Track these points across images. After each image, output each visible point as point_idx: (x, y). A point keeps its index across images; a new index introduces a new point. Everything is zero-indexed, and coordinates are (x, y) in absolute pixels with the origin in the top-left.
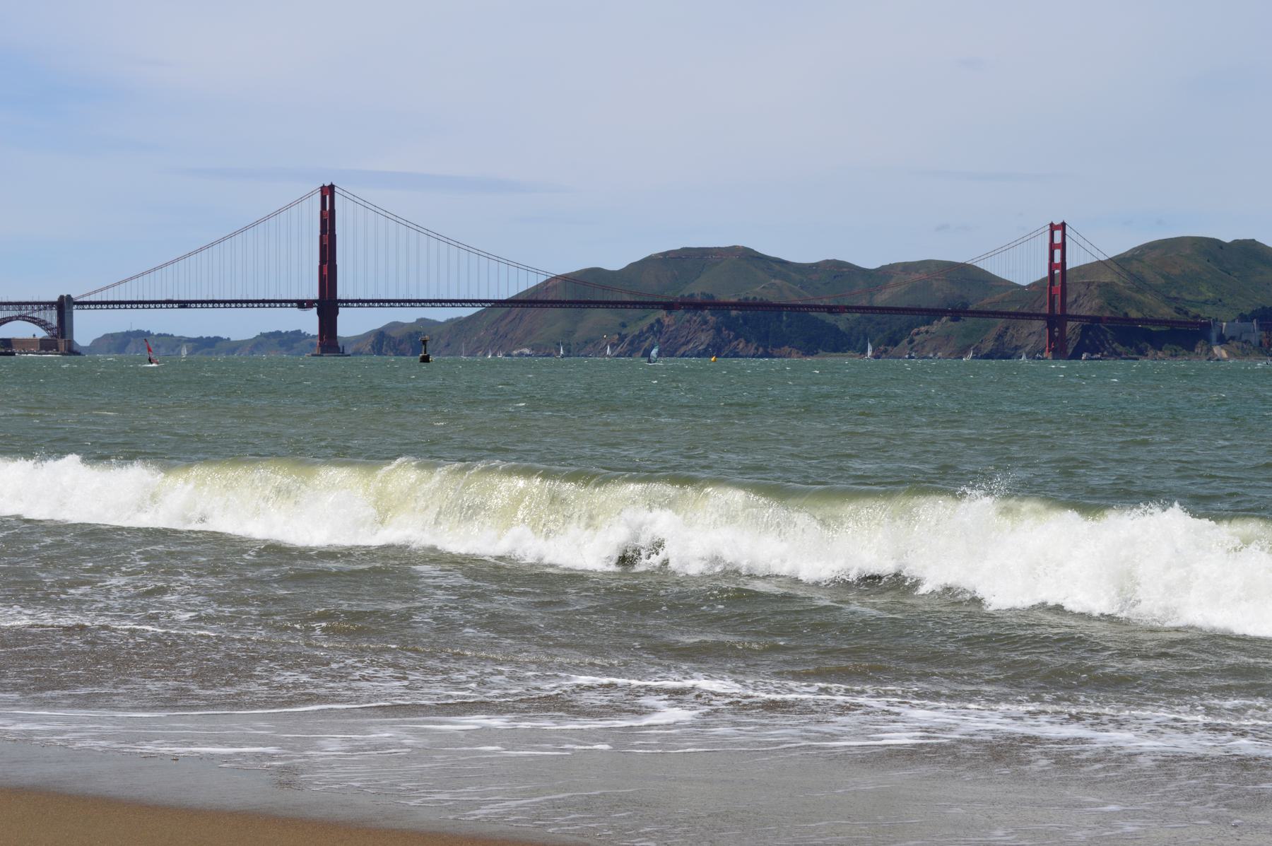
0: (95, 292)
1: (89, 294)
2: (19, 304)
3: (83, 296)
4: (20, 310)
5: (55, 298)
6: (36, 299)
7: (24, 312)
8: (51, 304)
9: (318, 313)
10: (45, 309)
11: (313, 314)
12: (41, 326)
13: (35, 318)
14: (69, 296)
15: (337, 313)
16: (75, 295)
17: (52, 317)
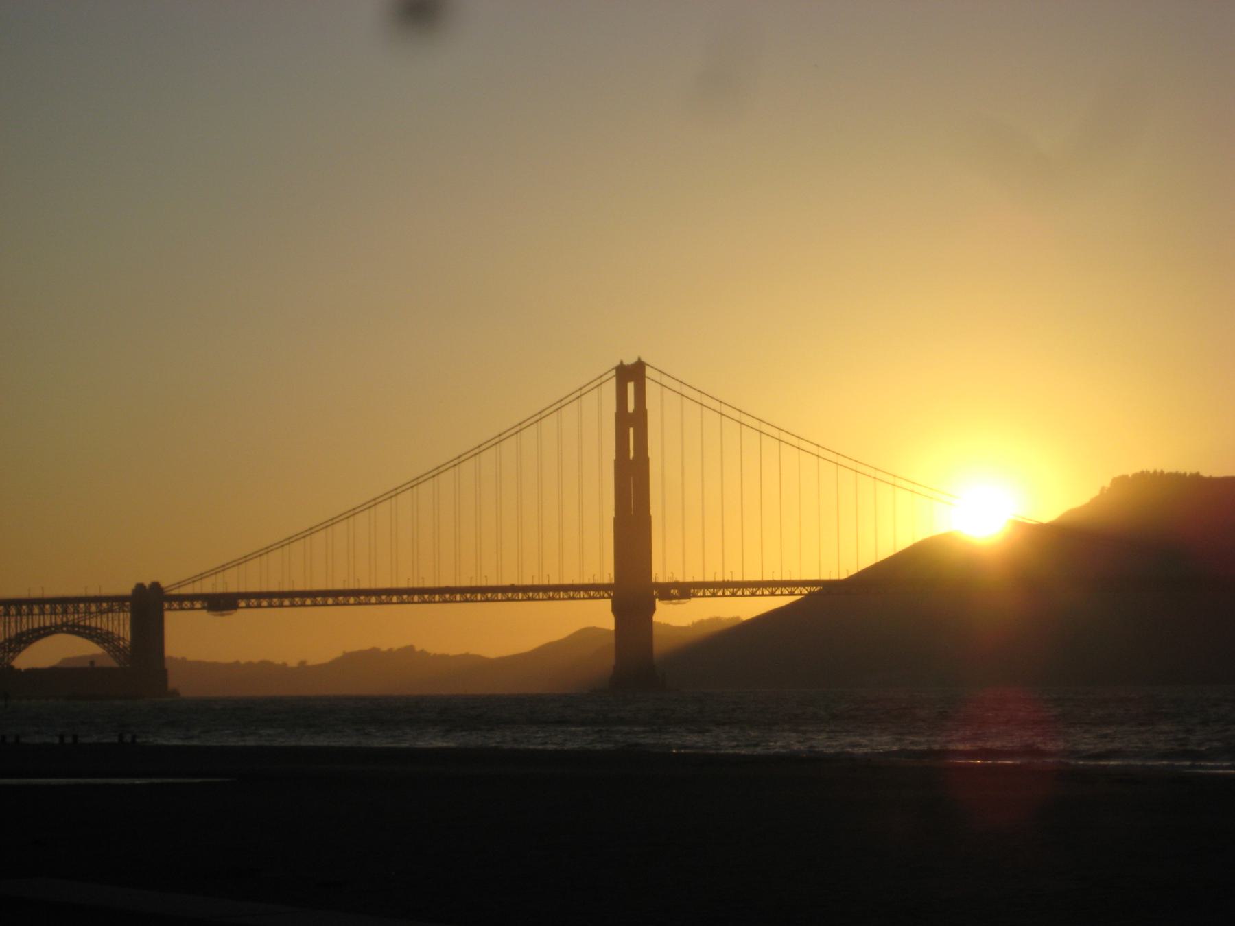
0: (202, 576)
1: (193, 580)
2: (64, 601)
3: (180, 584)
4: (65, 612)
5: (126, 589)
6: (93, 592)
7: (71, 618)
8: (120, 600)
9: (616, 610)
10: (110, 610)
11: (606, 604)
12: (78, 634)
13: (89, 628)
14: (156, 586)
15: (652, 609)
16: (163, 584)
17: (121, 625)
